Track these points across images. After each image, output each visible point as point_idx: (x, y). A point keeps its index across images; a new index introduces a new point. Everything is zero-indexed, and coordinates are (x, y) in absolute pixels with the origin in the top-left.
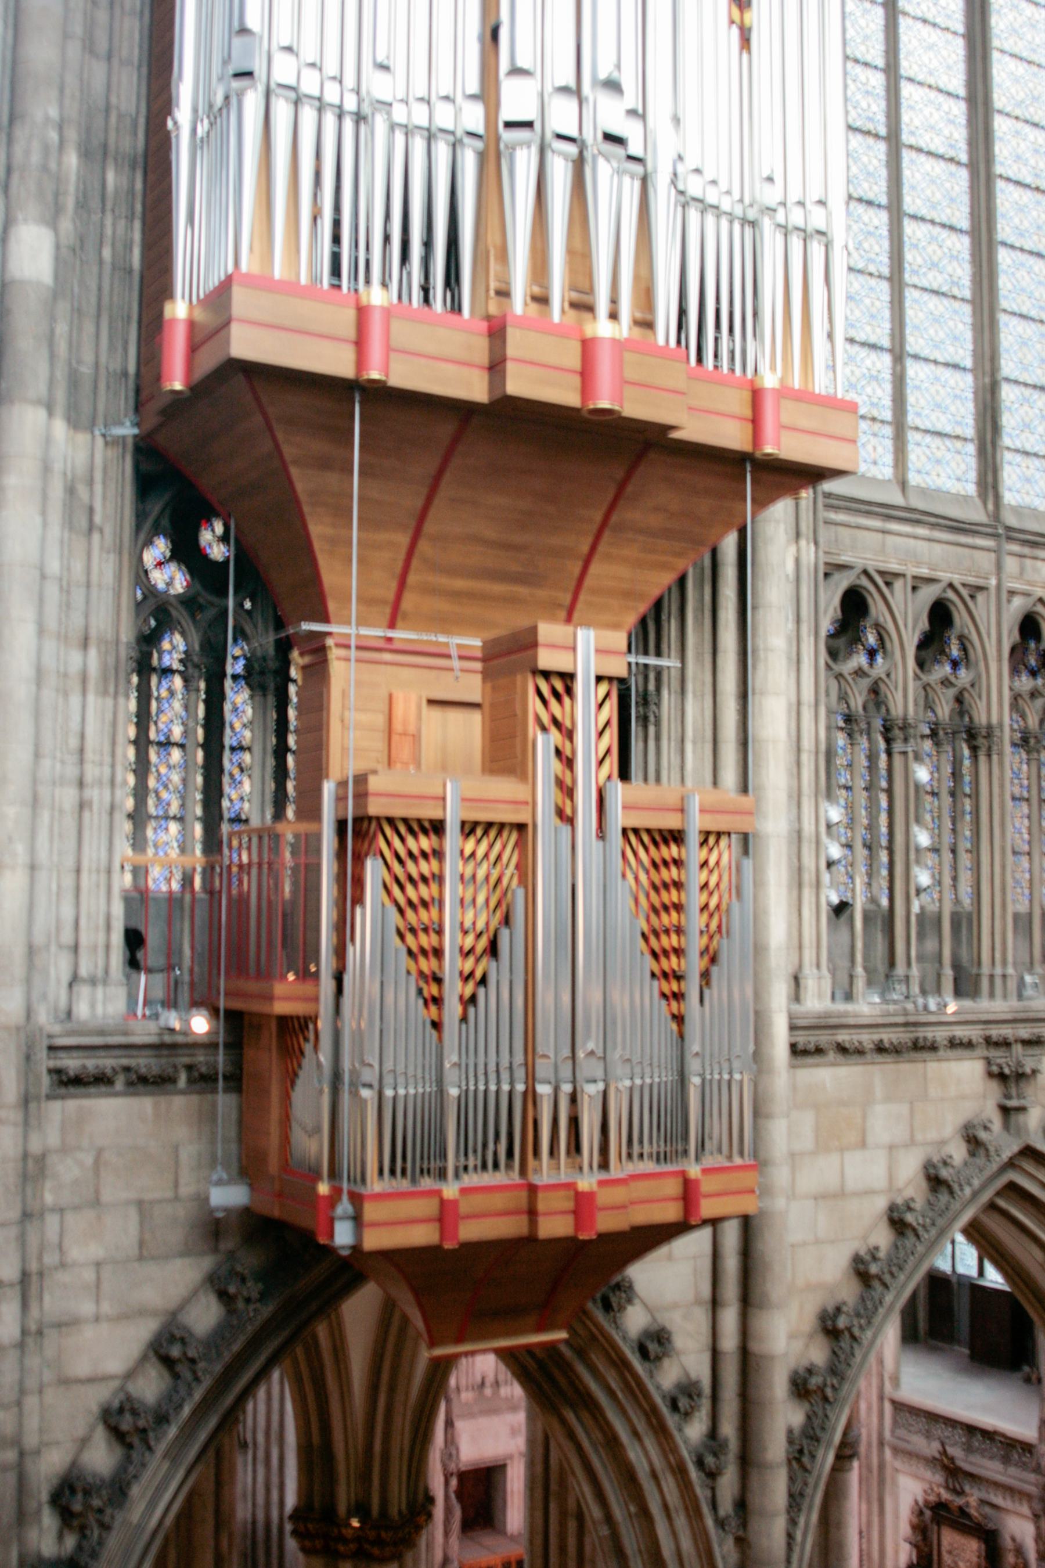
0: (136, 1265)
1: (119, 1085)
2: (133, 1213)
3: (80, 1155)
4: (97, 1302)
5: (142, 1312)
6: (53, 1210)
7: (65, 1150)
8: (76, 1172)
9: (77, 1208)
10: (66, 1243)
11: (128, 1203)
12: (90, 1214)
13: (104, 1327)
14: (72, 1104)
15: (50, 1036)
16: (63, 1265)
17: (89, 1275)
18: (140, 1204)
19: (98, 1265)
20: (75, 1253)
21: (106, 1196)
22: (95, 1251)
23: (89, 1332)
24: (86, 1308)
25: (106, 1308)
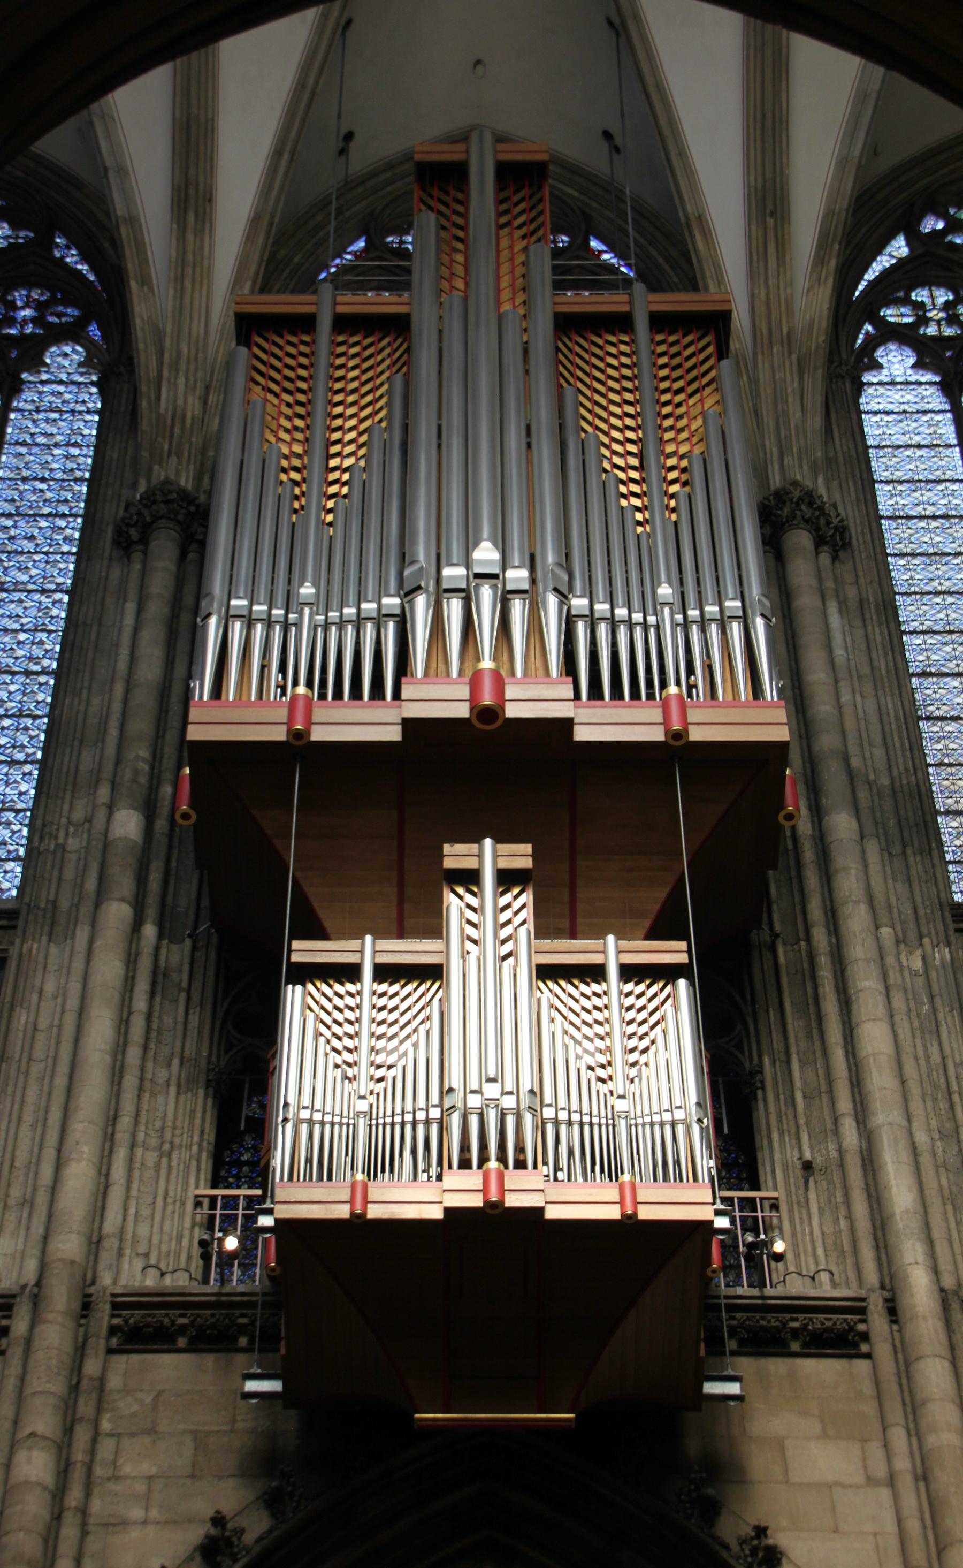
0: (189, 1481)
1: (182, 1342)
2: (188, 1439)
3: (139, 1395)
4: (147, 1510)
5: (191, 1520)
6: (109, 1435)
7: (126, 1391)
8: (135, 1407)
9: (133, 1435)
10: (120, 1461)
11: (183, 1432)
12: (147, 1440)
13: (151, 1529)
14: (135, 1358)
15: (113, 1295)
16: (115, 1478)
17: (141, 1487)
18: (195, 1433)
19: (150, 1479)
20: (127, 1469)
21: (163, 1426)
22: (147, 1468)
23: (135, 1534)
24: (136, 1513)
25: (154, 1513)
